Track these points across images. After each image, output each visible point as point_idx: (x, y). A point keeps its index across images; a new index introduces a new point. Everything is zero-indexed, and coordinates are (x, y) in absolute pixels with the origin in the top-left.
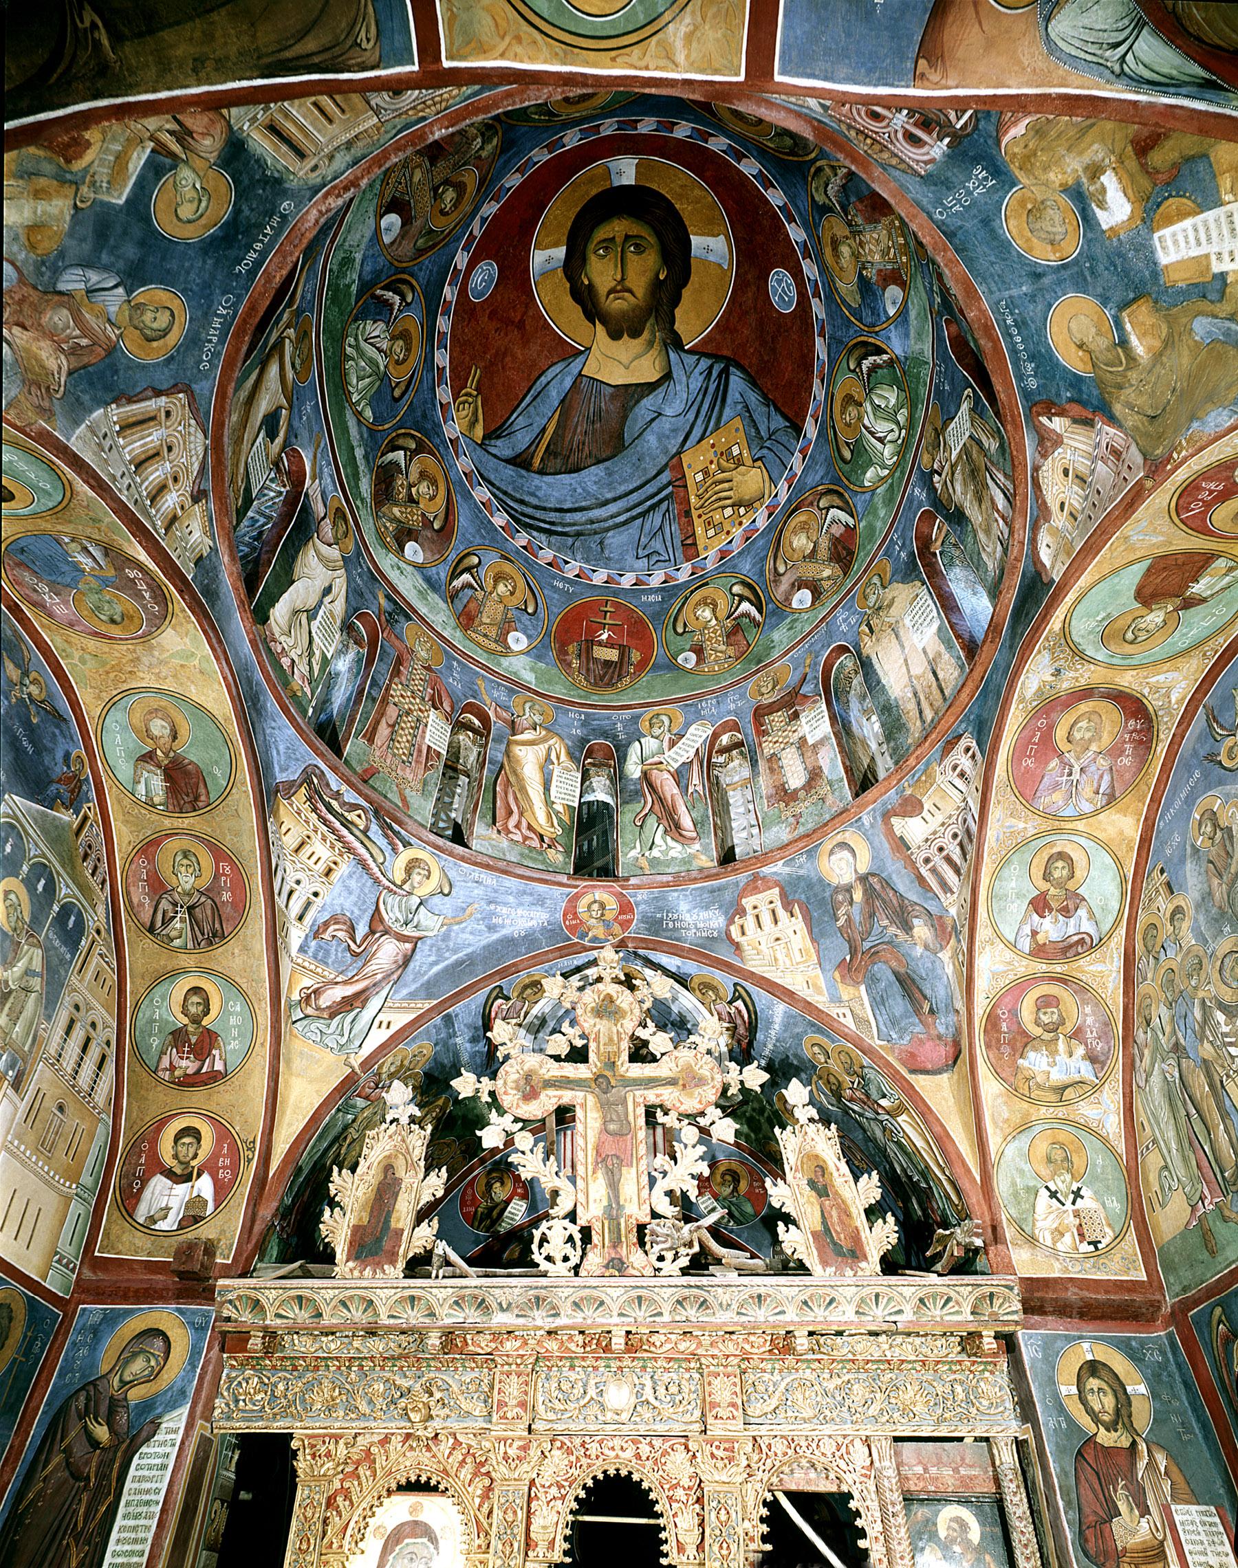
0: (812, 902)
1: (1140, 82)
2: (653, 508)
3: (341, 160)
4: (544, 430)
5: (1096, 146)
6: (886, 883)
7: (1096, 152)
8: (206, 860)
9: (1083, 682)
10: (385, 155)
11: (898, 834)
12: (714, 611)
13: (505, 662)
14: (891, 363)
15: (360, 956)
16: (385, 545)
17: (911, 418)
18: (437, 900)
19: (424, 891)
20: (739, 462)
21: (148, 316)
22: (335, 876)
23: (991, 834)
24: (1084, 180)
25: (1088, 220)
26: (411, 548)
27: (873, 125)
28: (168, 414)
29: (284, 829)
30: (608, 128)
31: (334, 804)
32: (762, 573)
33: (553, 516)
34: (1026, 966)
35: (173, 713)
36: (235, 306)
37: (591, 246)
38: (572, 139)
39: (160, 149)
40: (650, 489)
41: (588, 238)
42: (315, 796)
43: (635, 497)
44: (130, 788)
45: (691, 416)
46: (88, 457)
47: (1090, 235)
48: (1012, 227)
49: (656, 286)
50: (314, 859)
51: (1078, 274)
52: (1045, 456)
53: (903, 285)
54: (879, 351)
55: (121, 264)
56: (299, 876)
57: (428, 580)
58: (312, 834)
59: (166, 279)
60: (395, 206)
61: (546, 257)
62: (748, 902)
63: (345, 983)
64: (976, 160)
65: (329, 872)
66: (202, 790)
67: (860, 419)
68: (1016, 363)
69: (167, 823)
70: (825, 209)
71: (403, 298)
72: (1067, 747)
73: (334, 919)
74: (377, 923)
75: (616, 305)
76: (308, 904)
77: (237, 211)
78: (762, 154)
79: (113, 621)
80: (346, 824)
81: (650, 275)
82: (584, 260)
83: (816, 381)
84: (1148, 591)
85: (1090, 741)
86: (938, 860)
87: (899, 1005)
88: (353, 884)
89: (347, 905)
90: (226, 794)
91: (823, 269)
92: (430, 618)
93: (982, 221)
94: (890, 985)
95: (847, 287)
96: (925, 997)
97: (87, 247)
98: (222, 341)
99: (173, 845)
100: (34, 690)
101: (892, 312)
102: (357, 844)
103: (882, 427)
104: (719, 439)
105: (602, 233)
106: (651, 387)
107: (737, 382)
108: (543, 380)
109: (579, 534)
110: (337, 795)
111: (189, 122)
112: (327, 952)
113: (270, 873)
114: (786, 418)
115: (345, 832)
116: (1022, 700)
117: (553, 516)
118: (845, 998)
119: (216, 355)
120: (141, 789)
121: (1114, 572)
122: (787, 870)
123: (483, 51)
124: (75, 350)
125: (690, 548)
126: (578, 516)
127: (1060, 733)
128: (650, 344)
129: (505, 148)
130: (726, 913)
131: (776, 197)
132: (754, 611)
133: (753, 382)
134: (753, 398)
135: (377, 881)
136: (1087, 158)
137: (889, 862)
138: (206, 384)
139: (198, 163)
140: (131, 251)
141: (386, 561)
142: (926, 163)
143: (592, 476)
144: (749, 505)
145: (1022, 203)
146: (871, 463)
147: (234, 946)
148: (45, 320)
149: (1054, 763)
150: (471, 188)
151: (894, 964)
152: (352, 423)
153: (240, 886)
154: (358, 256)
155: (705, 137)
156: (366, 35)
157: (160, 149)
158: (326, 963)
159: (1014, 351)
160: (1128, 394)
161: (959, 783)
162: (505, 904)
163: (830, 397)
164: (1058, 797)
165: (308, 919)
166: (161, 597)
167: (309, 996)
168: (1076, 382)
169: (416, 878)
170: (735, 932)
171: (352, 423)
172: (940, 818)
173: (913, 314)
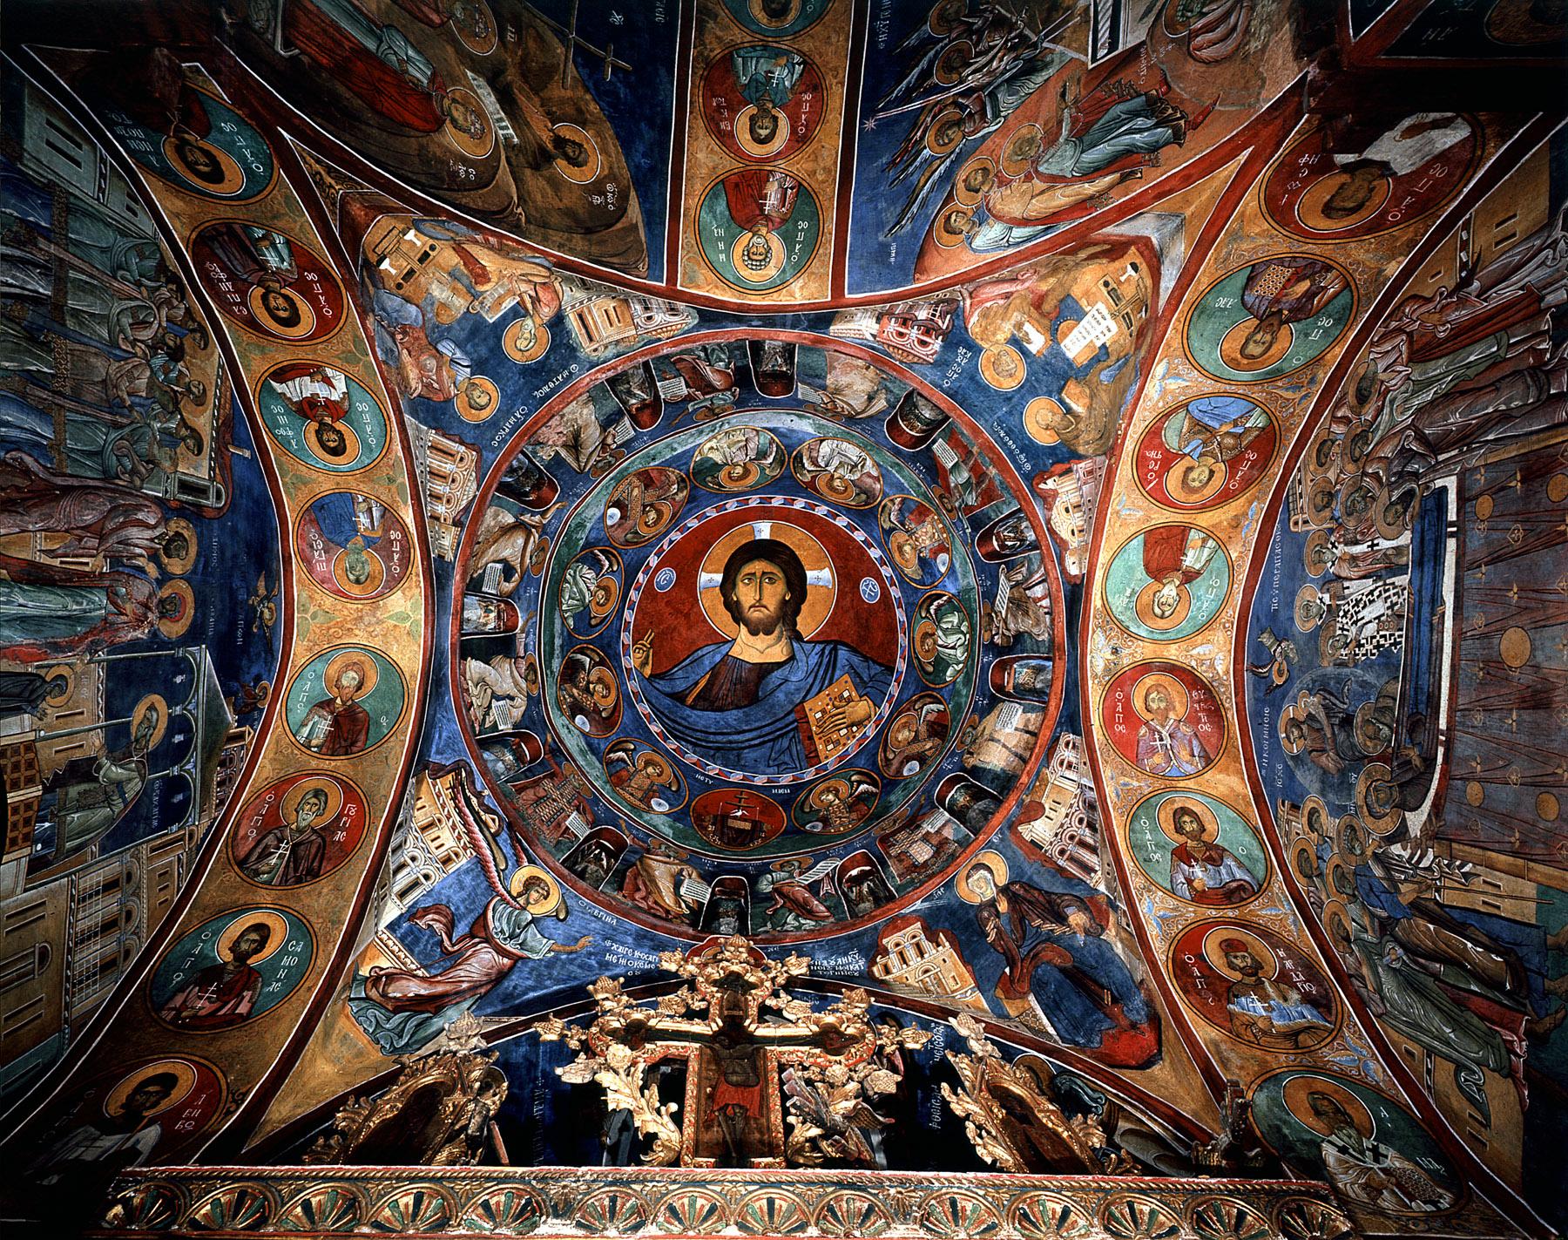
0: (957, 925)
1: (1018, 244)
2: (781, 736)
3: (611, 351)
4: (696, 683)
6: (1029, 886)
7: (1016, 316)
8: (336, 799)
9: (1139, 657)
10: (635, 357)
11: (1028, 838)
12: (836, 795)
13: (647, 817)
14: (949, 601)
15: (454, 959)
16: (560, 709)
17: (972, 627)
18: (550, 923)
19: (537, 910)
20: (850, 700)
21: (476, 393)
22: (452, 868)
23: (1109, 790)
25: (1025, 353)
26: (579, 719)
27: (899, 340)
28: (462, 459)
29: (419, 804)
30: (754, 502)
31: (474, 801)
32: (875, 763)
33: (699, 735)
34: (1191, 913)
35: (367, 667)
36: (527, 415)
37: (740, 577)
38: (732, 506)
39: (521, 304)
40: (779, 725)
41: (738, 571)
42: (457, 786)
43: (767, 729)
44: (298, 712)
45: (810, 680)
46: (410, 432)
48: (988, 376)
49: (784, 603)
50: (437, 843)
51: (1029, 389)
52: (1050, 509)
53: (946, 550)
54: (940, 596)
55: (475, 356)
56: (417, 853)
57: (589, 744)
58: (444, 819)
59: (496, 378)
60: (617, 504)
61: (710, 578)
62: (889, 942)
63: (423, 979)
65: (447, 861)
66: (362, 737)
67: (935, 642)
68: (1014, 461)
69: (314, 763)
70: (892, 529)
71: (611, 565)
72: (1148, 716)
73: (436, 908)
74: (479, 931)
75: (755, 615)
76: (415, 884)
77: (547, 357)
78: (848, 511)
79: (358, 581)
80: (478, 820)
81: (779, 597)
82: (734, 585)
83: (900, 635)
84: (1153, 565)
85: (1167, 710)
86: (1071, 848)
87: (1076, 1006)
88: (468, 880)
89: (455, 898)
90: (382, 740)
91: (895, 568)
92: (587, 769)
94: (1059, 985)
95: (912, 570)
96: (1102, 987)
97: (463, 335)
98: (511, 434)
99: (311, 783)
100: (267, 614)
101: (943, 569)
102: (484, 844)
103: (952, 640)
104: (835, 689)
105: (748, 569)
106: (779, 665)
107: (843, 653)
108: (700, 653)
109: (718, 749)
110: (479, 795)
111: (541, 294)
112: (417, 940)
113: (391, 826)
114: (881, 665)
115: (476, 829)
116: (1095, 676)
117: (699, 735)
118: (1013, 1013)
119: (504, 441)
120: (305, 731)
121: (1122, 548)
122: (926, 904)
123: (698, 287)
124: (428, 386)
125: (812, 758)
126: (719, 738)
127: (1138, 704)
128: (779, 639)
129: (691, 499)
130: (866, 957)
131: (859, 536)
132: (871, 788)
133: (854, 650)
134: (856, 660)
135: (492, 886)
137: (1026, 866)
138: (491, 456)
139: (538, 320)
140: (483, 351)
141: (559, 721)
143: (733, 716)
144: (860, 724)
145: (988, 359)
146: (949, 665)
147: (325, 886)
148: (423, 358)
149: (1143, 730)
150: (667, 516)
151: (1058, 961)
152: (558, 622)
153: (358, 829)
154: (589, 525)
155: (813, 507)
156: (643, 268)
157: (521, 304)
158: (411, 952)
159: (1010, 453)
160: (1084, 437)
161: (1068, 774)
162: (622, 944)
163: (911, 640)
164: (1158, 759)
165: (410, 899)
166: (406, 561)
167: (379, 978)
168: (1052, 451)
169: (534, 895)
170: (877, 971)
171: (558, 622)
172: (1063, 811)
173: (957, 566)
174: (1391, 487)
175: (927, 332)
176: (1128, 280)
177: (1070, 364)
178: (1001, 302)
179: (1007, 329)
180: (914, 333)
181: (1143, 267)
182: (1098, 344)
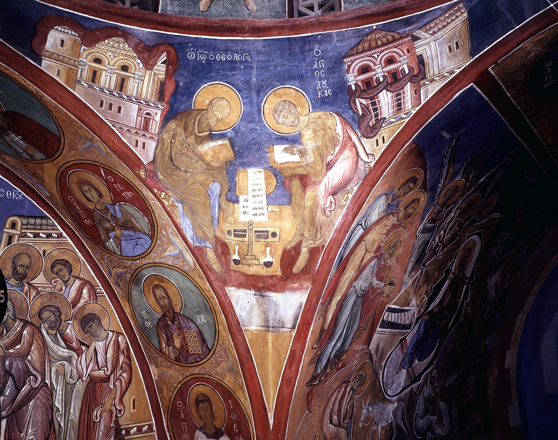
5: (313, 159)
24: (301, 147)
25: (282, 139)
27: (386, 54)
47: (273, 136)
64: (335, 94)
93: (302, 75)
136: (310, 152)
142: (349, 66)
175: (368, 83)
176: (264, 252)
177: (245, 165)
178: (329, 158)
179: (309, 141)
180: (379, 73)
181: (263, 271)
182: (242, 198)
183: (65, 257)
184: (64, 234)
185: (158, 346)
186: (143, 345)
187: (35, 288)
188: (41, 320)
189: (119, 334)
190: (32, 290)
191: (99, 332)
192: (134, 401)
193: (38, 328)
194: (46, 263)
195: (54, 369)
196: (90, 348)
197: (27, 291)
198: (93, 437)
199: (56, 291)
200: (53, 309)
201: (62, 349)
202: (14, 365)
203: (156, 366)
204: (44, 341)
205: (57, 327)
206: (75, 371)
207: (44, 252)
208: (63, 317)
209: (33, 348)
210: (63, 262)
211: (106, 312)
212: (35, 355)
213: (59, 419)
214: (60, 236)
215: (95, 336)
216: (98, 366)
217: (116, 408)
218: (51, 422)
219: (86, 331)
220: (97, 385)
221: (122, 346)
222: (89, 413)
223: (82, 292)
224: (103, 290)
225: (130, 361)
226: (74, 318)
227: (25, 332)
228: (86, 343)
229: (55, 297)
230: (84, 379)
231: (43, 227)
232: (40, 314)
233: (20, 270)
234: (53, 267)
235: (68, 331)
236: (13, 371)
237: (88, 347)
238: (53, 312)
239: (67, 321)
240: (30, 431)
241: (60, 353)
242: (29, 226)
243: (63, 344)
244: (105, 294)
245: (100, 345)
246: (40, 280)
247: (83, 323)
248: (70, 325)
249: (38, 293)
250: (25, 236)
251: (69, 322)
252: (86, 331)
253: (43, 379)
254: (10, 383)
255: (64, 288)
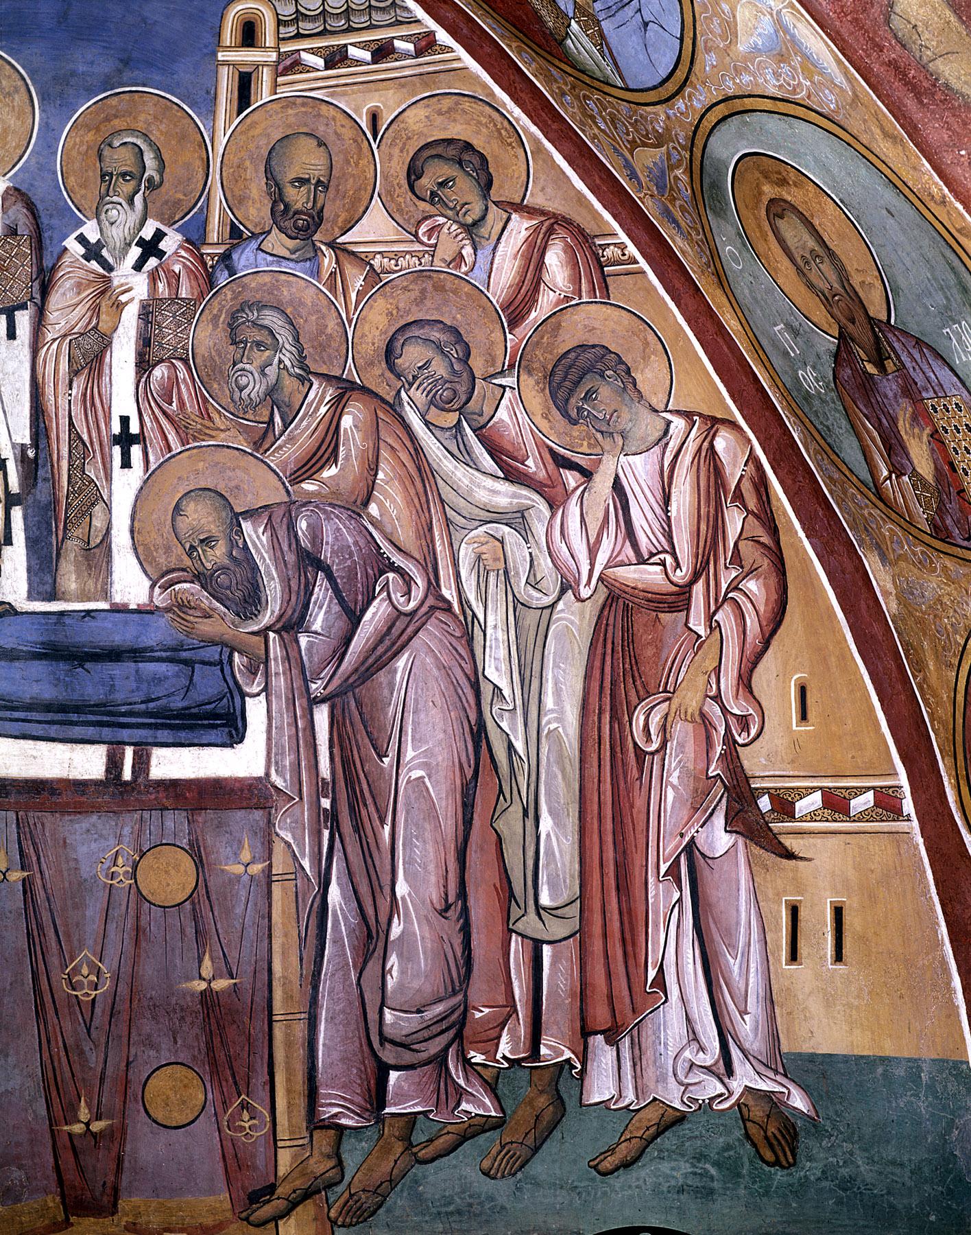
174: (280, 517)
183: (457, 130)
184: (443, 36)
185: (865, 475)
186: (819, 466)
187: (362, 260)
188: (398, 376)
189: (714, 423)
190: (350, 270)
191: (625, 415)
192: (803, 691)
193: (391, 406)
194: (389, 163)
195: (466, 555)
196: (597, 478)
197: (333, 274)
198: (639, 802)
199: (439, 265)
200: (436, 335)
201: (489, 482)
202: (328, 537)
203: (883, 558)
204: (417, 451)
205: (459, 401)
206: (545, 563)
207: (374, 118)
208: (478, 364)
209: (381, 475)
210: (451, 152)
211: (651, 337)
212: (394, 501)
213: (507, 727)
214: (426, 44)
215: (611, 432)
216: (635, 546)
217: (724, 710)
218: (479, 734)
219: (574, 413)
220: (641, 619)
221: (734, 471)
222: (615, 716)
223: (541, 264)
224: (632, 249)
225: (774, 531)
226: (519, 363)
227: (347, 422)
228: (578, 459)
229: (439, 288)
230: (585, 592)
231: (358, 20)
232: (390, 354)
233: (298, 198)
234: (414, 173)
235: (502, 414)
236: (326, 554)
237: (587, 474)
238: (439, 348)
239: (493, 376)
240: (409, 753)
241: (482, 496)
242: (306, 27)
243: (487, 462)
244: (643, 264)
245: (640, 470)
246: (374, 229)
247: (560, 386)
248: (508, 393)
249: (374, 276)
250: (293, 65)
251: (503, 381)
252: (574, 413)
253: (433, 585)
254: (321, 591)
255: (467, 251)
